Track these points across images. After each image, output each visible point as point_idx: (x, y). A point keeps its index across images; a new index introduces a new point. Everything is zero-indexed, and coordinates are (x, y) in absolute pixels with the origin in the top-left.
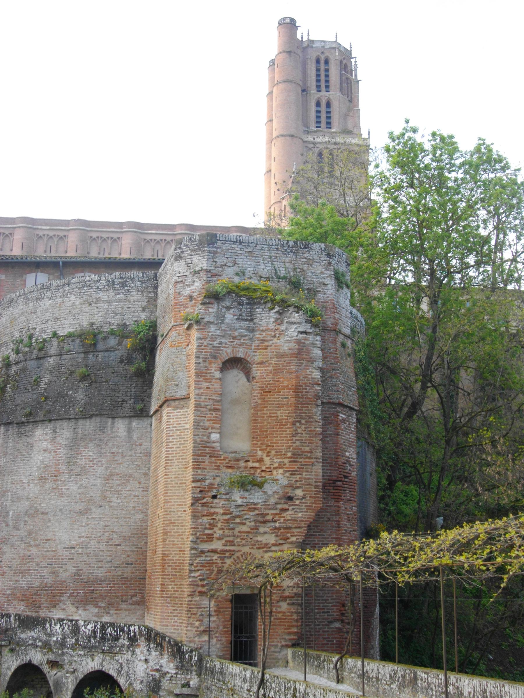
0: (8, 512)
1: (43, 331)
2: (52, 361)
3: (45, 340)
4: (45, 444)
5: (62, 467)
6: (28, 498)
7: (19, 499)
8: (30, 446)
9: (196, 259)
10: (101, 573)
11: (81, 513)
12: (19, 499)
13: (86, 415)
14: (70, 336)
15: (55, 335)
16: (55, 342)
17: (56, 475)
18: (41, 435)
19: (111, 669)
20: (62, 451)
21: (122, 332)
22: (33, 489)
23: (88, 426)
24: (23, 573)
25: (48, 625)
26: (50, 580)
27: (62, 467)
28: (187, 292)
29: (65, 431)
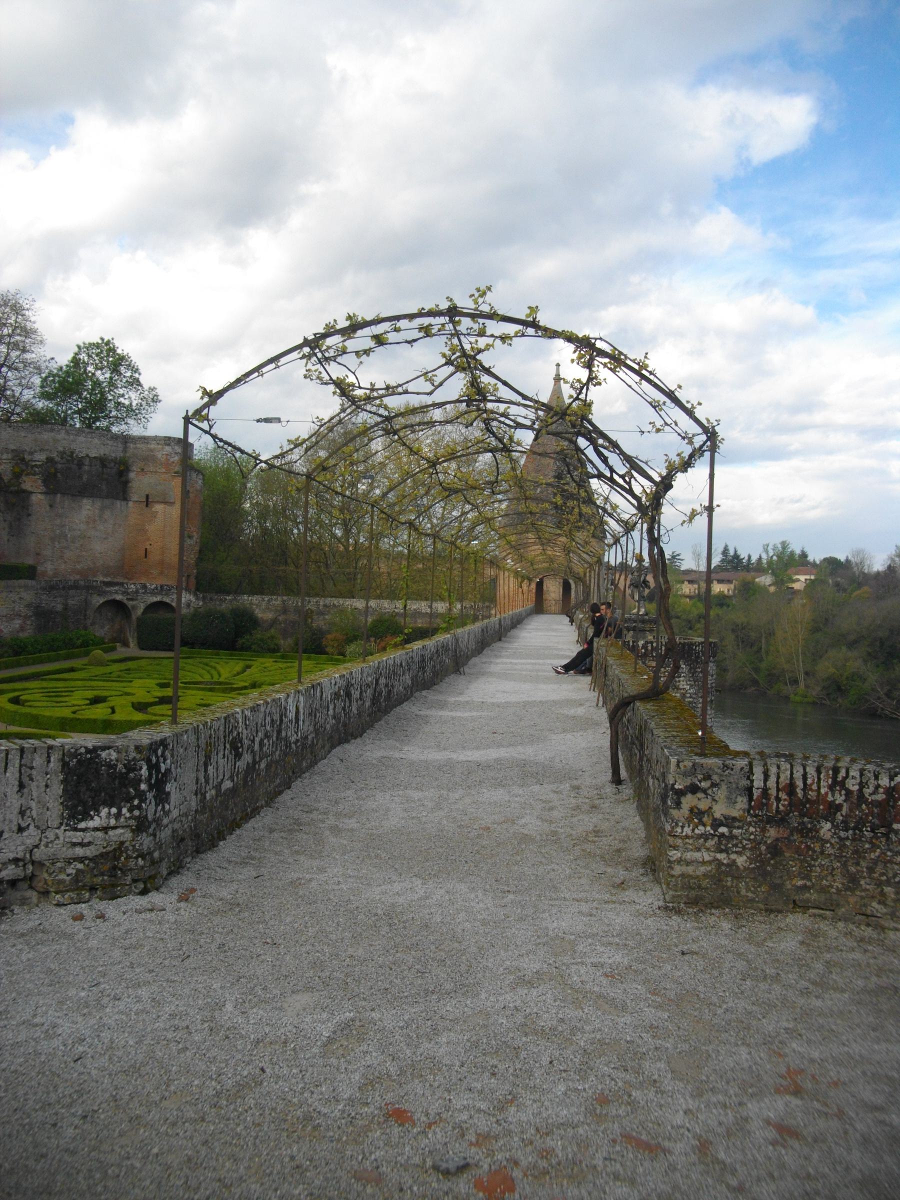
2: (86, 468)
3: (82, 457)
4: (88, 507)
5: (97, 518)
7: (74, 530)
9: (176, 448)
10: (111, 564)
11: (105, 539)
13: (107, 497)
14: (95, 458)
15: (87, 456)
16: (88, 459)
17: (95, 521)
18: (86, 501)
20: (97, 511)
21: (114, 461)
22: (83, 527)
23: (107, 502)
24: (79, 562)
26: (92, 566)
27: (97, 518)
28: (172, 460)
29: (98, 503)
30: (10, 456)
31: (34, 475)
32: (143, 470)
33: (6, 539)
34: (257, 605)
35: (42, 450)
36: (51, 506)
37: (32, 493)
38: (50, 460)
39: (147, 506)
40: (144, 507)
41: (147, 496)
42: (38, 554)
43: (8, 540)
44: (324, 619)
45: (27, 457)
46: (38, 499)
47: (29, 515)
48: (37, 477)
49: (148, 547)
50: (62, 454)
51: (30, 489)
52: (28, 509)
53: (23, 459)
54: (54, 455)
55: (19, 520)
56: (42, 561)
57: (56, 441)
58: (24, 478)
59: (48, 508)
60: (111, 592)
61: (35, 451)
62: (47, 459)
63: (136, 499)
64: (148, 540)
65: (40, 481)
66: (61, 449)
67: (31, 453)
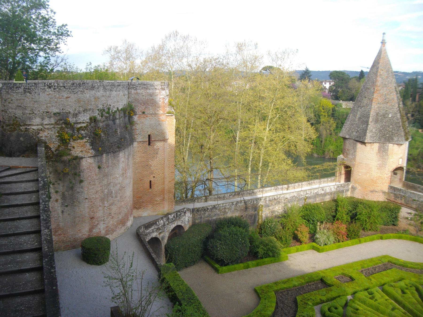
0: (112, 192)
1: (114, 107)
6: (119, 183)
8: (118, 161)
12: (116, 185)
19: (180, 224)
25: (158, 223)
30: (53, 121)
31: (82, 139)
32: (144, 113)
33: (60, 212)
34: (229, 209)
35: (85, 110)
36: (99, 167)
37: (82, 158)
38: (93, 120)
39: (149, 144)
40: (147, 146)
41: (149, 136)
42: (92, 218)
43: (63, 212)
44: (269, 209)
45: (71, 120)
46: (88, 163)
47: (81, 181)
48: (85, 140)
49: (152, 179)
50: (102, 111)
51: (80, 155)
52: (79, 176)
53: (67, 123)
54: (96, 114)
55: (72, 188)
56: (96, 222)
57: (97, 99)
58: (72, 143)
59: (97, 169)
60: (149, 233)
61: (79, 113)
62: (91, 119)
63: (140, 140)
64: (152, 173)
65: (88, 145)
66: (101, 107)
67: (76, 115)
